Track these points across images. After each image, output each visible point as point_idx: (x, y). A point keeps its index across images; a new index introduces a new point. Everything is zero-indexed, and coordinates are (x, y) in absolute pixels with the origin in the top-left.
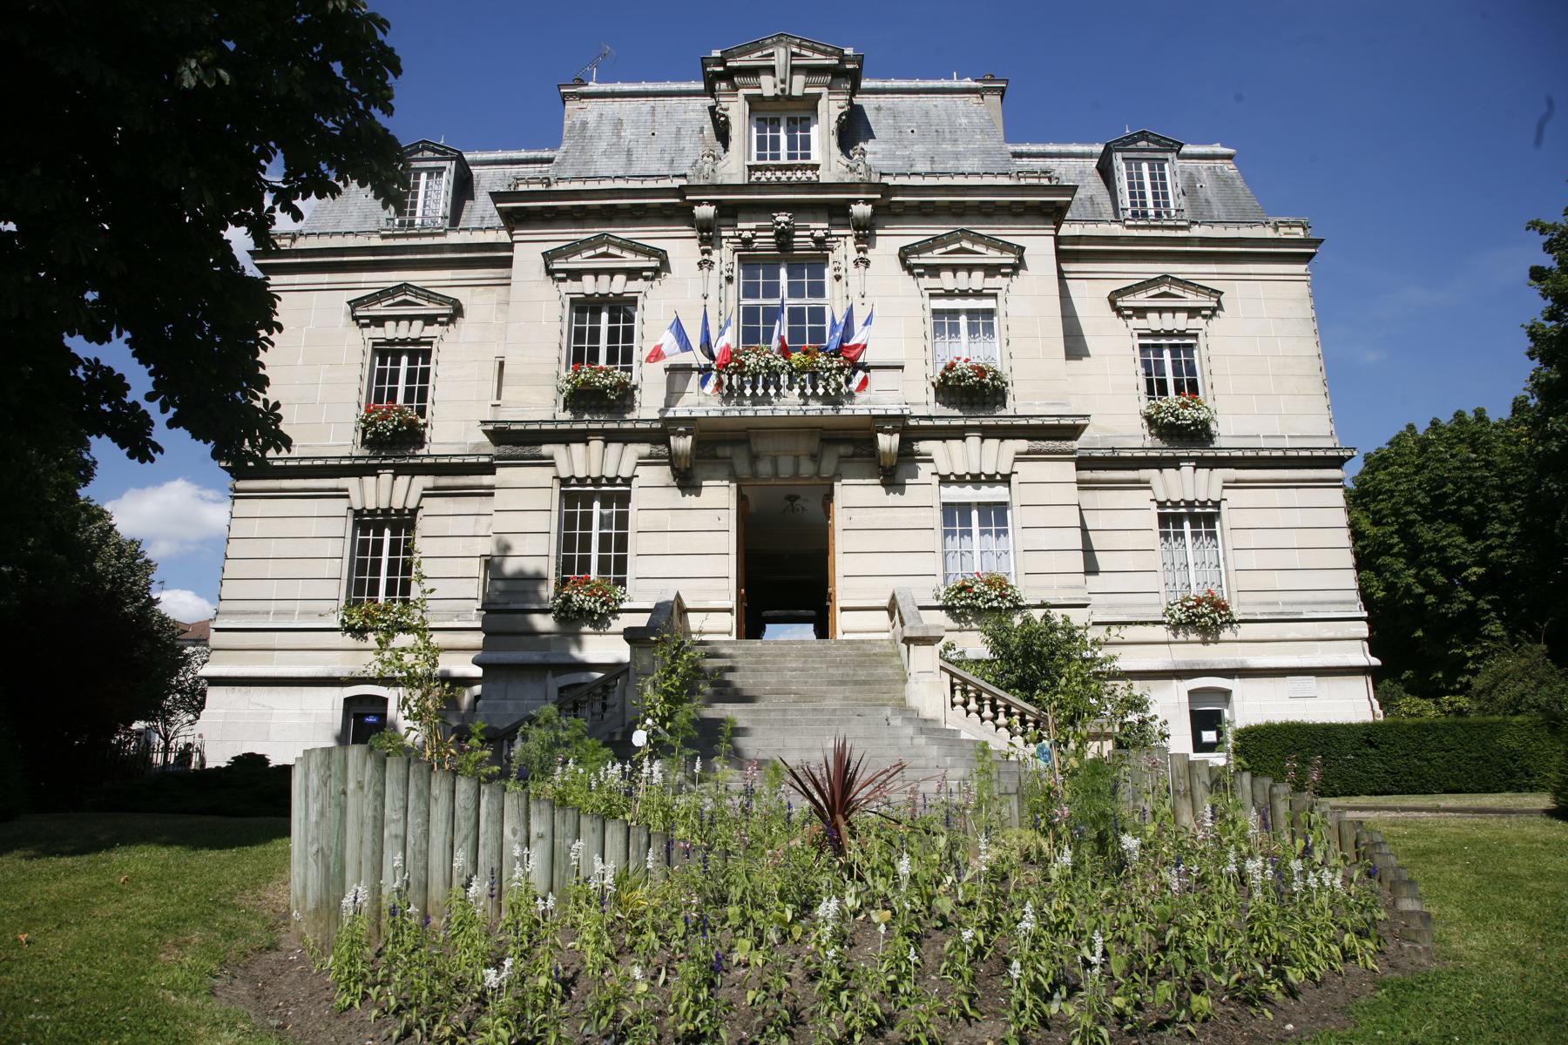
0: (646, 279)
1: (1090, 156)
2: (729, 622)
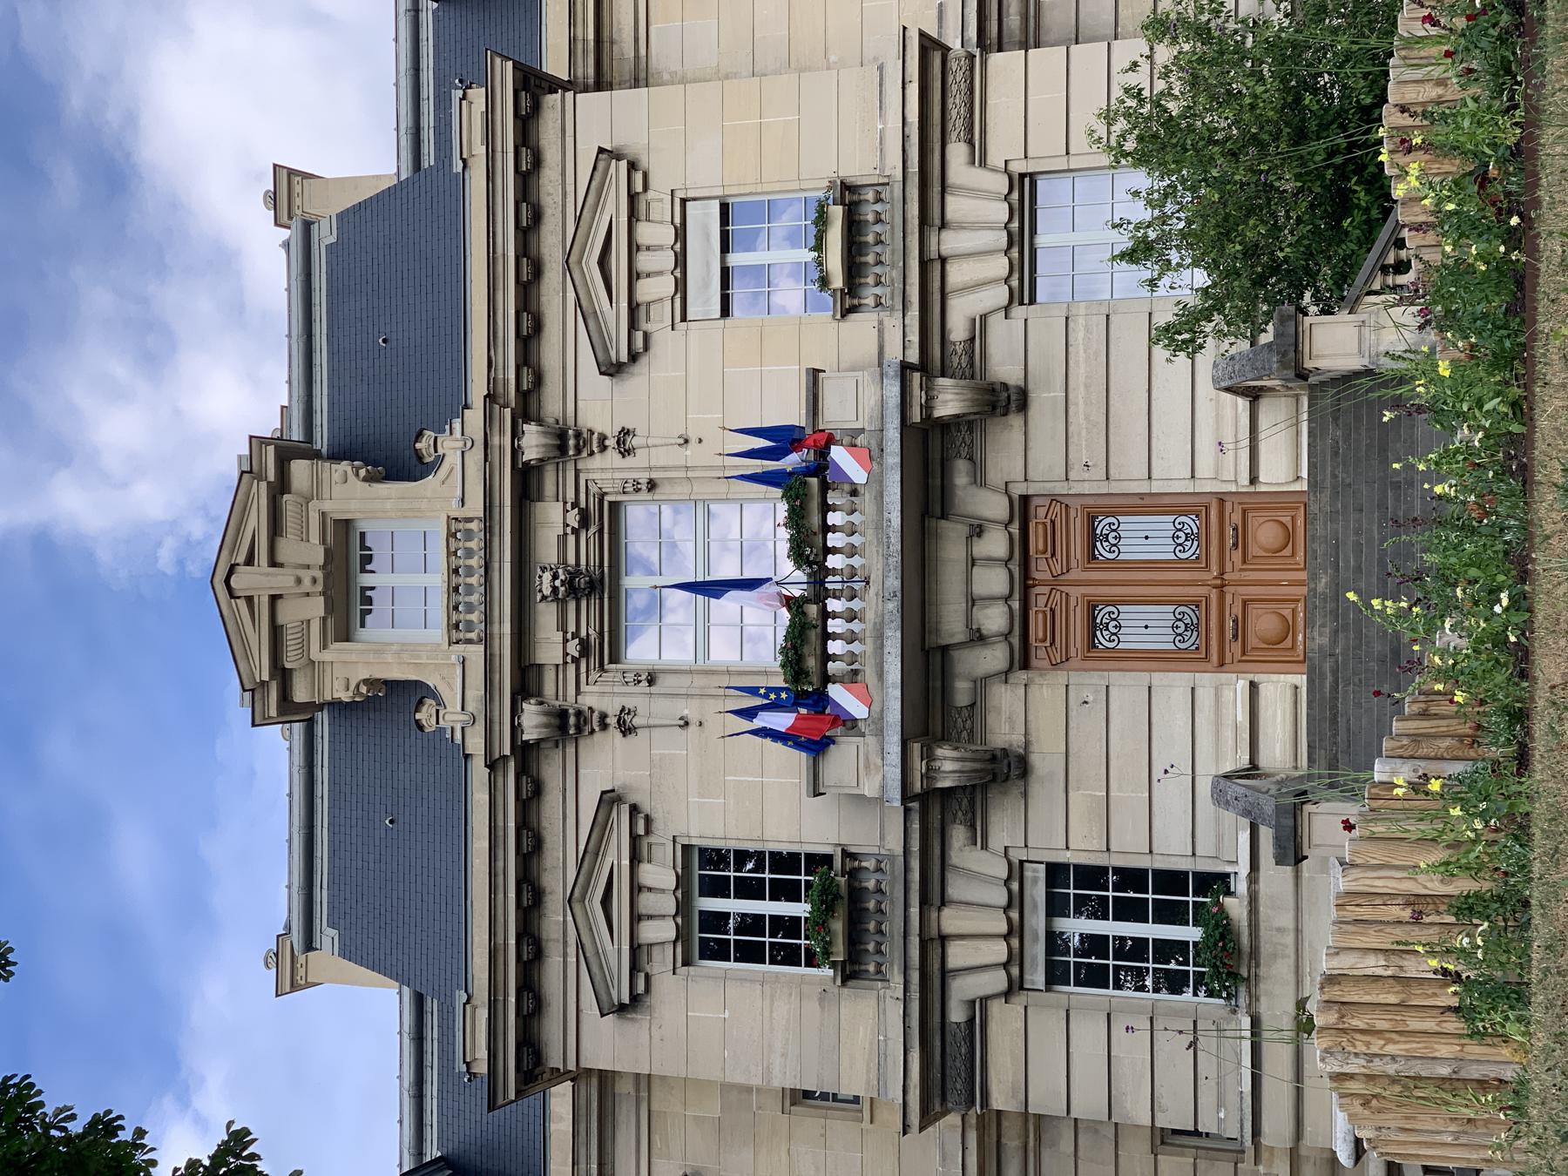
0: (648, 831)
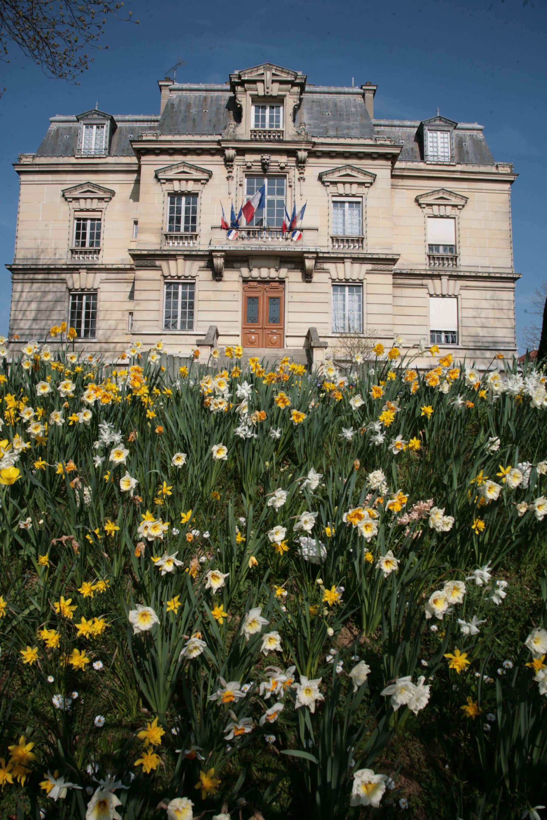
1: (414, 127)
2: (238, 341)
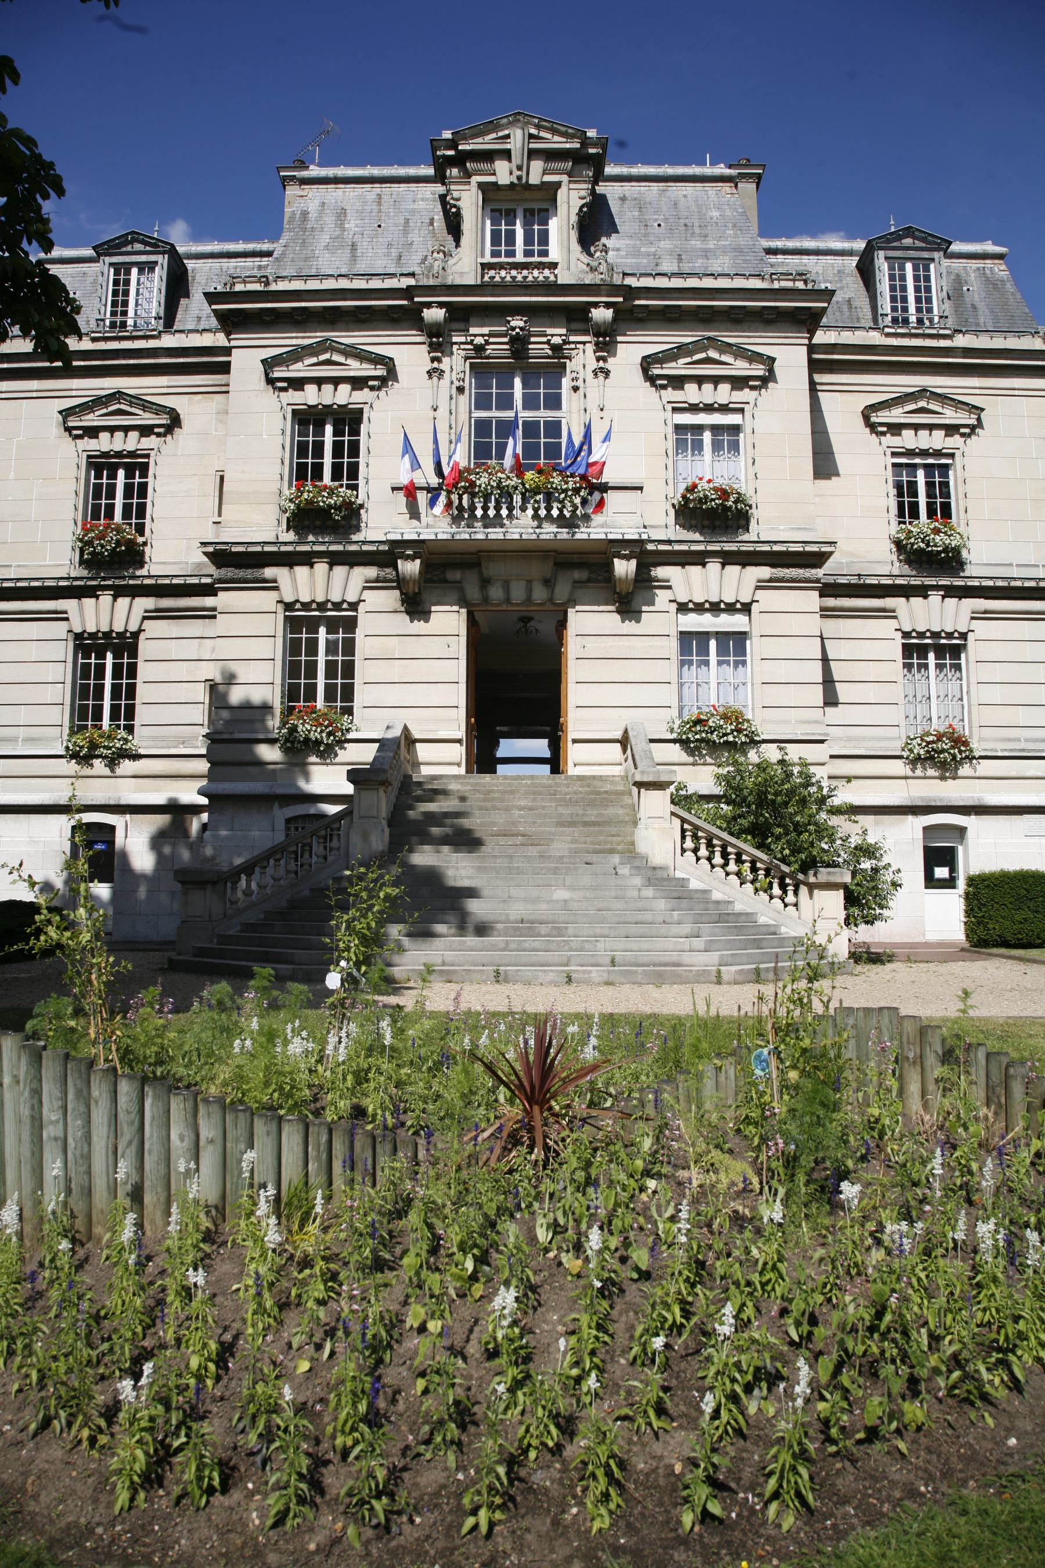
0: (372, 388)
1: (850, 253)
2: (458, 752)
